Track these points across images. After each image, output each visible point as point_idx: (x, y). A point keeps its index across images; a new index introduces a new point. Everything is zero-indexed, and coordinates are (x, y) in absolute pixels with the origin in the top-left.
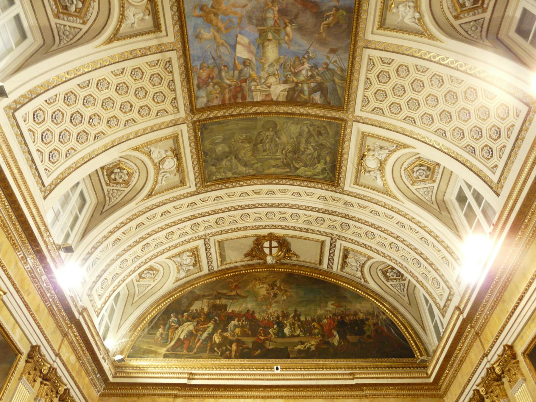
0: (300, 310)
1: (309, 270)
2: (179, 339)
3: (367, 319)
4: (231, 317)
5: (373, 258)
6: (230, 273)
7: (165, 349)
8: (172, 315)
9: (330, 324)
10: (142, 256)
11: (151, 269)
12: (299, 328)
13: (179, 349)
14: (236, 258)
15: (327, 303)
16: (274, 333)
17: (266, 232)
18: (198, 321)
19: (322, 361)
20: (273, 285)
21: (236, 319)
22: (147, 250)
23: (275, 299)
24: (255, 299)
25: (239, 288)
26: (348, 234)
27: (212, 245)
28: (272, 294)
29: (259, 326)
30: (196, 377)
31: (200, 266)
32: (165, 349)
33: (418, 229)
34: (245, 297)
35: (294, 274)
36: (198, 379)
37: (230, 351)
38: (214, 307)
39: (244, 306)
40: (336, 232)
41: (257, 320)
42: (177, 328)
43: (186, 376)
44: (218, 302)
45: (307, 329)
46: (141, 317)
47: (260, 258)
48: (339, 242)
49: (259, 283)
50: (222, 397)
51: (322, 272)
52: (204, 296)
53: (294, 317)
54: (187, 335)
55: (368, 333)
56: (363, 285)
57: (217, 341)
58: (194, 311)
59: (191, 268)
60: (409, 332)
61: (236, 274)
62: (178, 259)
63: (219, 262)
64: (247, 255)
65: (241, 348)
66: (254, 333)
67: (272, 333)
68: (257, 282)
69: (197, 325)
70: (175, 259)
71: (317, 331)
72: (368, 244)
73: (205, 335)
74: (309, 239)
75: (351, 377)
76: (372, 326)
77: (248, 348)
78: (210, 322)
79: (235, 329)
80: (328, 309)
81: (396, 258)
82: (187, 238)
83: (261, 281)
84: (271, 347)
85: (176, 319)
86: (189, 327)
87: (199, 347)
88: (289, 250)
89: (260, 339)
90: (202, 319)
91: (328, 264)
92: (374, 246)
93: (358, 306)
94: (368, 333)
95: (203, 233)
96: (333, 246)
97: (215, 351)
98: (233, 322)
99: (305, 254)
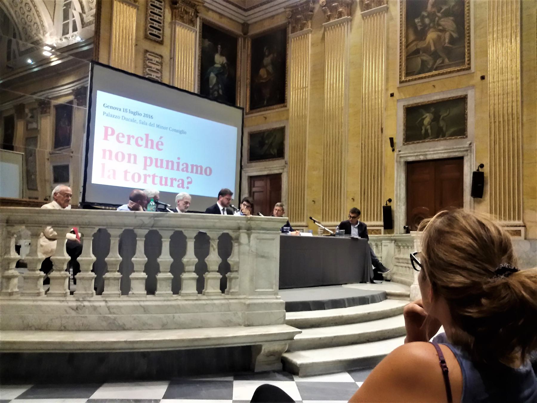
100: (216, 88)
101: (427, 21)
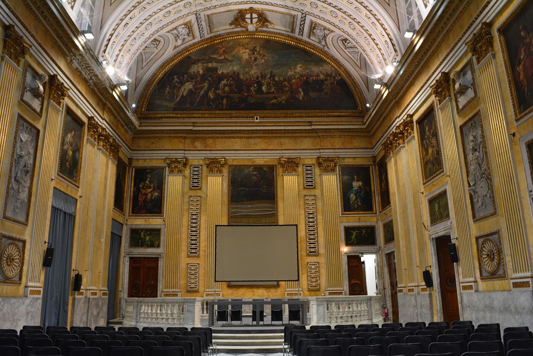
0: (274, 71)
3: (326, 80)
6: (218, 40)
7: (173, 104)
8: (175, 77)
11: (155, 40)
15: (296, 66)
16: (254, 91)
17: (247, 6)
18: (195, 82)
25: (227, 53)
26: (316, 12)
28: (253, 58)
31: (193, 35)
32: (173, 104)
33: (370, 16)
34: (232, 61)
37: (222, 104)
39: (231, 68)
41: (241, 80)
42: (180, 87)
44: (210, 65)
47: (243, 27)
51: (293, 38)
52: (199, 60)
53: (270, 78)
54: (188, 92)
55: (326, 91)
59: (186, 37)
61: (223, 41)
62: (175, 32)
63: (209, 31)
68: (241, 48)
70: (173, 32)
71: (287, 88)
76: (329, 85)
80: (297, 71)
82: (181, 14)
83: (244, 46)
84: (252, 102)
90: (199, 80)
94: (326, 91)
95: (195, 10)
96: (304, 20)
98: (223, 82)
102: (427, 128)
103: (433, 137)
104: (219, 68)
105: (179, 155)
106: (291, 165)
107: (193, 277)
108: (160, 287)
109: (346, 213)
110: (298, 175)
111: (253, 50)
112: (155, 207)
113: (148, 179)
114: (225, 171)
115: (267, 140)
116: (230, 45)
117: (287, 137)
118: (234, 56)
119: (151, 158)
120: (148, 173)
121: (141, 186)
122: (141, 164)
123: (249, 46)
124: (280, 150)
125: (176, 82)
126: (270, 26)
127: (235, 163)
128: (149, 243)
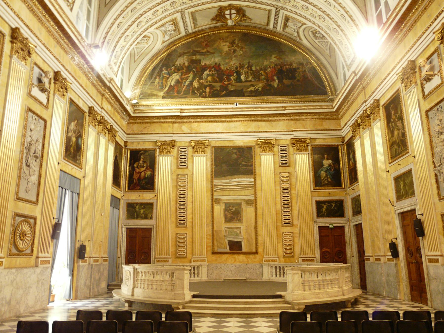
0: (252, 62)
1: (259, 30)
2: (171, 86)
3: (298, 68)
4: (204, 69)
5: (306, 24)
9: (272, 72)
10: (138, 31)
11: (145, 37)
12: (251, 75)
13: (171, 93)
14: (205, 23)
15: (271, 56)
16: (234, 80)
17: (226, 3)
19: (265, 98)
20: (232, 43)
21: (208, 70)
22: (140, 26)
23: (235, 54)
24: (220, 54)
25: (209, 46)
27: (187, 16)
28: (232, 51)
29: (224, 74)
30: (185, 111)
31: (179, 30)
33: (340, 8)
34: (213, 53)
35: (248, 34)
36: (186, 112)
37: (205, 92)
38: (192, 62)
39: (213, 60)
40: (280, 5)
42: (168, 78)
43: (179, 111)
44: (194, 57)
45: (257, 76)
46: (142, 71)
47: (223, 22)
48: (281, 12)
49: (223, 41)
50: (202, 122)
52: (184, 53)
53: (247, 68)
55: (298, 78)
56: (298, 42)
57: (196, 86)
58: (179, 65)
60: (326, 77)
61: (205, 36)
62: (163, 29)
63: (193, 26)
64: (213, 19)
65: (212, 90)
66: (221, 80)
67: (232, 79)
69: (182, 75)
70: (160, 29)
71: (263, 77)
72: (303, 14)
73: (188, 82)
74: (259, 8)
75: (283, 109)
76: (301, 73)
77: (217, 90)
78: (190, 73)
79: (207, 77)
80: (272, 61)
81: (323, 27)
82: (168, 13)
83: (224, 39)
84: (232, 89)
85: (166, 72)
86: (176, 77)
87: (185, 91)
88: (244, 15)
89: (225, 84)
90: (184, 71)
91: (274, 25)
92: (308, 16)
93: (293, 58)
94: (298, 78)
95: (179, 8)
96: (277, 14)
97: (195, 93)
99: (257, 17)
100: (326, 178)
101: (393, 124)
102: (393, 112)
103: (399, 120)
104: (202, 59)
105: (168, 138)
106: (267, 145)
107: (181, 245)
108: (153, 254)
109: (317, 188)
110: (274, 155)
111: (232, 43)
112: (148, 184)
113: (142, 160)
114: (209, 151)
115: (246, 123)
116: (212, 38)
117: (263, 121)
118: (216, 49)
119: (144, 141)
120: (141, 154)
121: (135, 165)
122: (135, 147)
123: (229, 39)
124: (257, 132)
125: (165, 74)
126: (248, 21)
127: (217, 144)
128: (143, 215)
